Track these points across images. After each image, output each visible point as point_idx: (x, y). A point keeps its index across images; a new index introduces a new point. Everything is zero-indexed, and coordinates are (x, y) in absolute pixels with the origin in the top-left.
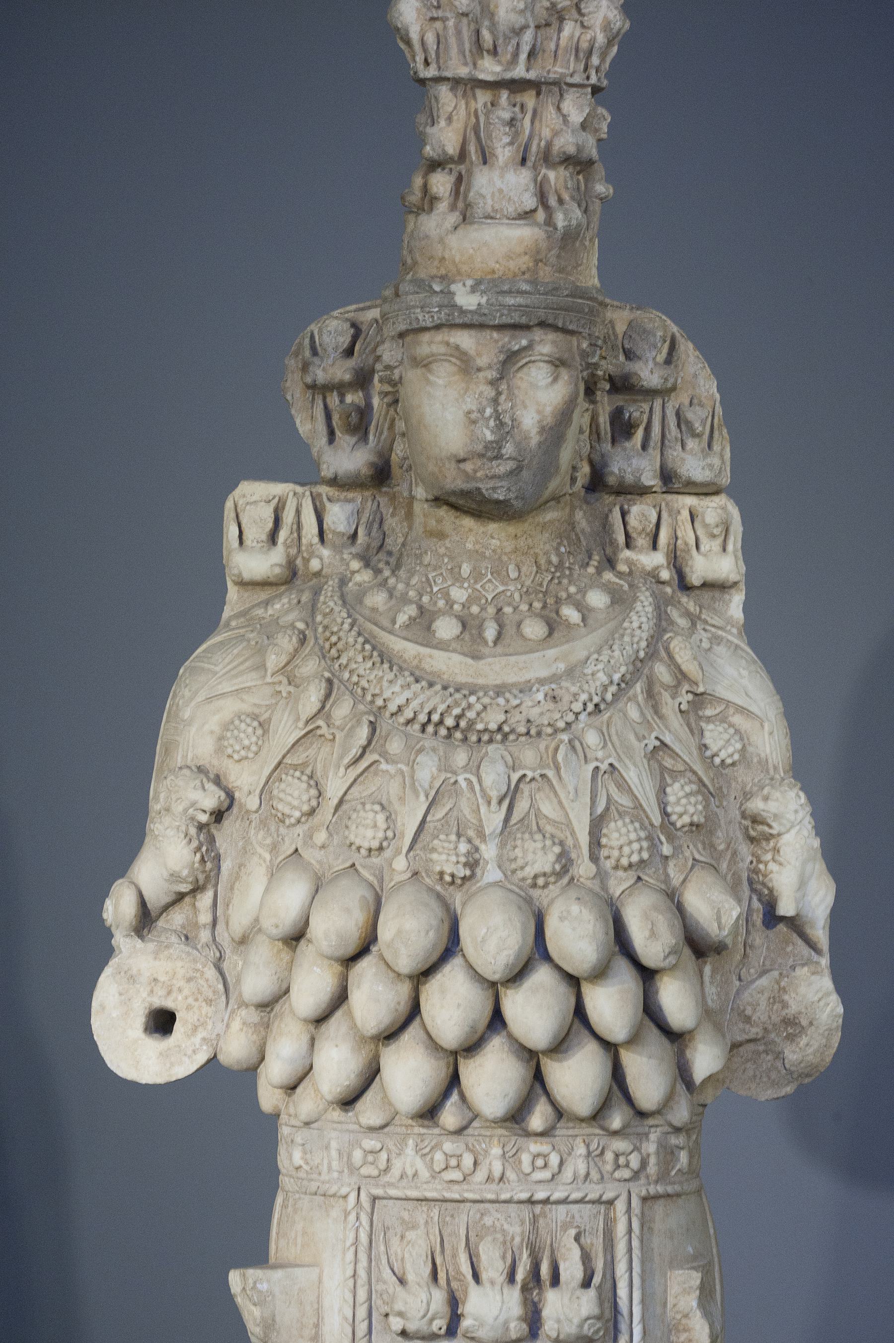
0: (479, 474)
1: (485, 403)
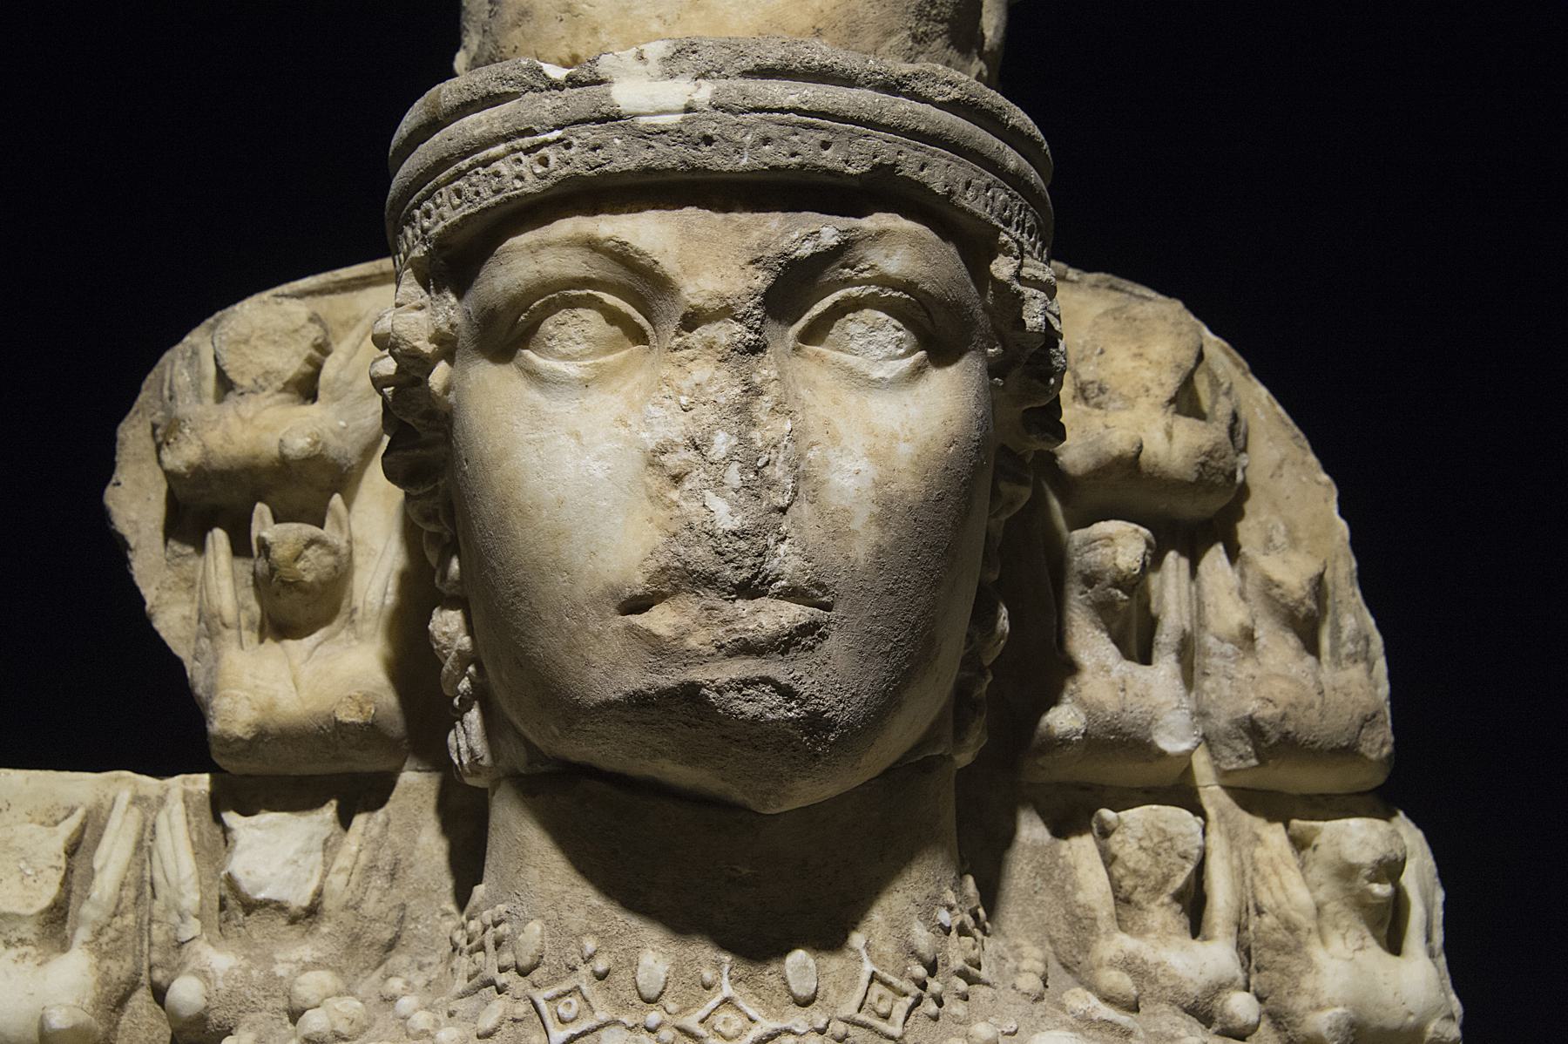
0: (692, 642)
1: (708, 416)
